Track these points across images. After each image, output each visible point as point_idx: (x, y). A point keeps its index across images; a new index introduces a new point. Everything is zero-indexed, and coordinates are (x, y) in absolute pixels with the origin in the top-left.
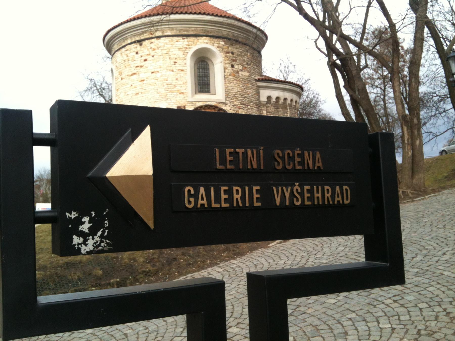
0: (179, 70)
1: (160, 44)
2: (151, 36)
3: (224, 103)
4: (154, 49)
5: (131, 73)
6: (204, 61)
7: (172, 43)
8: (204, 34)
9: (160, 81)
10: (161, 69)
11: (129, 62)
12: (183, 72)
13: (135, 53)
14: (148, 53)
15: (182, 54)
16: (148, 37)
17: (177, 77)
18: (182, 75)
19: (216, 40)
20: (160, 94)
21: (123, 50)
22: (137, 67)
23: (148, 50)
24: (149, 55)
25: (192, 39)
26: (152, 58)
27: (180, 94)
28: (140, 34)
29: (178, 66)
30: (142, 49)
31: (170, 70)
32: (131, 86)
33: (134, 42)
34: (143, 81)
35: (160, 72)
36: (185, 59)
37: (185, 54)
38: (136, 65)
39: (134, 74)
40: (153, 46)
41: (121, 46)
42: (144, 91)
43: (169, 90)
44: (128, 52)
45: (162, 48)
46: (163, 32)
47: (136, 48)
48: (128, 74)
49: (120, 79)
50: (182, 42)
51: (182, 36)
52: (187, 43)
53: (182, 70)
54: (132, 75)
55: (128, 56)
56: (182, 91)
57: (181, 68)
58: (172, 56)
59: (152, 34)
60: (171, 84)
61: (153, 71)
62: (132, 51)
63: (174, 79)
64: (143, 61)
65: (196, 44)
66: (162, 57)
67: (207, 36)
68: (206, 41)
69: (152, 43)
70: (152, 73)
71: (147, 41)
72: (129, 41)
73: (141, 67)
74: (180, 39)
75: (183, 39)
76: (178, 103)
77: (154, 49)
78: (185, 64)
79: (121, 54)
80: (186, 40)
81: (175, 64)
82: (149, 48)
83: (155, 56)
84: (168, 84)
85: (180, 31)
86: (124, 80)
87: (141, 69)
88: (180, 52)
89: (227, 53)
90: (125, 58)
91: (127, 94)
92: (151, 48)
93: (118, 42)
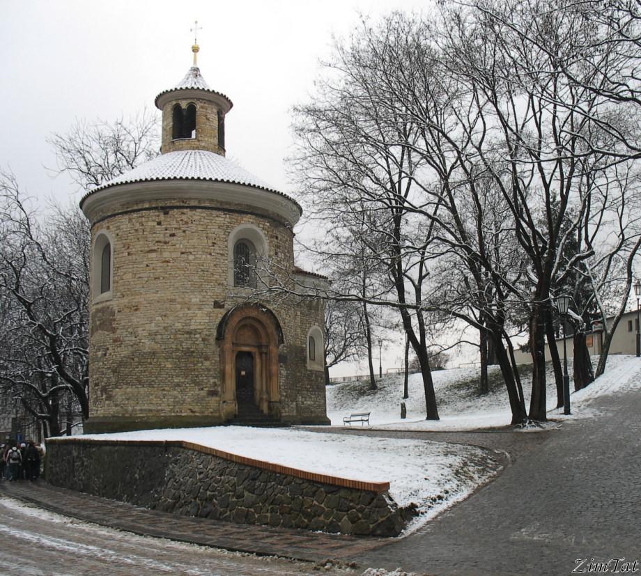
1: (195, 218)
2: (182, 204)
4: (186, 223)
5: (147, 249)
7: (211, 218)
8: (249, 211)
9: (193, 266)
10: (196, 250)
11: (145, 233)
13: (156, 223)
16: (178, 204)
20: (192, 283)
21: (135, 215)
22: (157, 242)
23: (177, 222)
24: (179, 229)
25: (235, 216)
26: (183, 234)
27: (219, 284)
28: (166, 199)
30: (169, 220)
32: (147, 266)
33: (156, 208)
34: (168, 262)
35: (193, 253)
36: (226, 241)
38: (157, 239)
40: (184, 217)
41: (129, 209)
42: (167, 276)
44: (143, 219)
45: (198, 223)
46: (199, 202)
47: (158, 216)
48: (143, 249)
50: (223, 219)
51: (224, 210)
52: (229, 220)
53: (222, 255)
55: (143, 225)
57: (221, 252)
58: (210, 235)
59: (183, 202)
60: (207, 271)
61: (183, 250)
63: (212, 265)
64: (168, 235)
65: (240, 223)
66: (196, 234)
67: (252, 214)
69: (183, 213)
70: (182, 253)
71: (175, 210)
72: (147, 206)
73: (166, 243)
77: (186, 223)
78: (226, 247)
79: (130, 219)
80: (228, 216)
81: (213, 246)
82: (179, 219)
83: (187, 232)
84: (203, 271)
85: (222, 203)
86: (134, 257)
88: (220, 230)
89: (272, 237)
90: (137, 226)
91: (139, 276)
92: (182, 220)
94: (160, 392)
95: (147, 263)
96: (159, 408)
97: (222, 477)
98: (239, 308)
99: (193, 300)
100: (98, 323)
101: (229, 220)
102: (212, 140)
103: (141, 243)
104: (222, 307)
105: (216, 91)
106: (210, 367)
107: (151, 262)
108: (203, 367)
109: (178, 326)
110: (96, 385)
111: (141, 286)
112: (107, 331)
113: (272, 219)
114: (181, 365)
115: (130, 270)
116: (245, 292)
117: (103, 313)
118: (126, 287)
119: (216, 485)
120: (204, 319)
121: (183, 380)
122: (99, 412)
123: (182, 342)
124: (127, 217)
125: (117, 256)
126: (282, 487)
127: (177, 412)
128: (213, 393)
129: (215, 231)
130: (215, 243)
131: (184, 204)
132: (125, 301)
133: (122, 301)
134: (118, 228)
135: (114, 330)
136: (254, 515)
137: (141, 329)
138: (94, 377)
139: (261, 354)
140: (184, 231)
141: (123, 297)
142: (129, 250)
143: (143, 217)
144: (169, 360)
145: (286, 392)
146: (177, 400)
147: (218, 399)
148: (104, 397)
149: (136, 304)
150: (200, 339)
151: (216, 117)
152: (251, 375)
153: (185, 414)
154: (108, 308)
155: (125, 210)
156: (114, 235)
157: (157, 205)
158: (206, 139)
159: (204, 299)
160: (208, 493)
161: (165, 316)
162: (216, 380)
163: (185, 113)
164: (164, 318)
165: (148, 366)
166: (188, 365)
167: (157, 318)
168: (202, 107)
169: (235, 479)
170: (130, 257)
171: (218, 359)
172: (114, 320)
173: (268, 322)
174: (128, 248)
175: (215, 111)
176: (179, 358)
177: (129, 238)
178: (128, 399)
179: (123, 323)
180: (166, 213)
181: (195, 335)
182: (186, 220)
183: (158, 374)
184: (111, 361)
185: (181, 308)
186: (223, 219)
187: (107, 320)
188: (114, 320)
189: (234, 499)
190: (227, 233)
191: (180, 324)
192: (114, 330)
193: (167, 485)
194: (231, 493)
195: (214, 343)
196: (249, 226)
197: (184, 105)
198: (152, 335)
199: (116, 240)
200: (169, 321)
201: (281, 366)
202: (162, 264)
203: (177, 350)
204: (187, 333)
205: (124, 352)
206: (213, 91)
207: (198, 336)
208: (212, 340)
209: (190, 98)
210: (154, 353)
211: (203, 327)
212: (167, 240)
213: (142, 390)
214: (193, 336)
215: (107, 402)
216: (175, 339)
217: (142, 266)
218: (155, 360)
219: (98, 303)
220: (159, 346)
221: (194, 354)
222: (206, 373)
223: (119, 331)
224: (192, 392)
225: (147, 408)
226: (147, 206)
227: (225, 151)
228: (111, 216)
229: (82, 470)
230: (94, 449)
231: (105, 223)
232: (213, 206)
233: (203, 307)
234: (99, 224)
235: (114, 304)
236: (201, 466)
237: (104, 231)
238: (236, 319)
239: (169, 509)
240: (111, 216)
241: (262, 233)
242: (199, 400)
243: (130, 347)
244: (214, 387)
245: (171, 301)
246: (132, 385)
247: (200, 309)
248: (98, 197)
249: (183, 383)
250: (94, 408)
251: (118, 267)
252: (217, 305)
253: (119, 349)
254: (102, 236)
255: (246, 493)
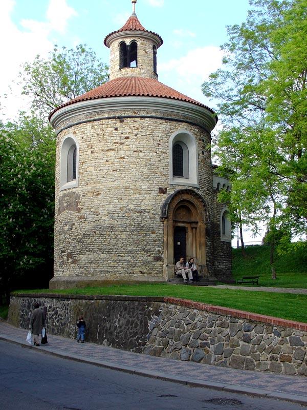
0: (162, 152)
2: (134, 115)
3: (198, 189)
4: (137, 129)
6: (179, 145)
12: (165, 155)
14: (130, 131)
15: (165, 136)
16: (131, 114)
17: (159, 159)
18: (165, 157)
19: (193, 127)
21: (96, 123)
22: (115, 143)
25: (174, 123)
27: (163, 175)
28: (121, 111)
29: (161, 149)
31: (153, 151)
32: (107, 161)
33: (114, 118)
34: (124, 158)
36: (168, 142)
37: (168, 137)
38: (115, 141)
39: (112, 150)
40: (135, 124)
41: (92, 119)
43: (152, 170)
45: (146, 129)
46: (147, 113)
47: (116, 124)
48: (103, 148)
49: (90, 152)
50: (165, 126)
51: (166, 119)
52: (169, 127)
54: (108, 150)
55: (103, 130)
56: (165, 173)
57: (164, 151)
59: (135, 113)
60: (154, 165)
61: (135, 149)
62: (109, 125)
68: (186, 127)
69: (135, 121)
70: (134, 151)
71: (129, 119)
73: (121, 144)
74: (163, 121)
75: (166, 122)
76: (160, 185)
77: (137, 129)
79: (93, 127)
80: (169, 124)
87: (121, 146)
88: (163, 134)
89: (200, 140)
90: (99, 131)
91: (100, 168)
92: (134, 127)
93: (88, 114)
94: (117, 258)
95: (107, 159)
96: (116, 269)
97: (213, 328)
98: (179, 193)
99: (143, 187)
100: (65, 205)
101: (169, 127)
102: (149, 68)
103: (102, 144)
104: (165, 192)
105: (153, 32)
106: (156, 238)
107: (110, 158)
108: (151, 239)
109: (132, 207)
110: (63, 252)
111: (102, 176)
112: (73, 211)
113: (201, 127)
114: (134, 237)
115: (93, 165)
116: (181, 183)
117: (70, 196)
118: (90, 177)
119: (207, 335)
120: (153, 202)
121: (135, 248)
122: (65, 273)
123: (134, 219)
124: (90, 124)
125: (82, 154)
126: (280, 339)
127: (130, 273)
128: (158, 259)
129: (158, 134)
130: (160, 144)
131: (136, 115)
132: (89, 187)
133: (86, 188)
134: (83, 133)
135: (79, 210)
136: (253, 362)
137: (102, 209)
138: (61, 246)
139: (192, 228)
140: (136, 135)
141: (87, 185)
142: (92, 150)
143: (103, 124)
144: (124, 233)
145: (210, 258)
146: (130, 263)
147: (161, 263)
148: (70, 261)
149: (98, 190)
150: (148, 217)
151: (152, 51)
152: (184, 244)
153: (136, 275)
154: (74, 193)
155: (89, 119)
156: (80, 138)
157: (114, 116)
158: (145, 67)
159: (151, 187)
160: (199, 341)
161: (121, 199)
162: (160, 249)
163: (128, 48)
164: (120, 201)
165: (107, 237)
166: (139, 237)
167: (115, 201)
168: (142, 44)
169: (228, 330)
170: (93, 155)
171: (162, 232)
172: (80, 202)
173: (199, 203)
174: (91, 148)
175: (151, 46)
176: (132, 232)
177: (92, 140)
178: (91, 263)
179: (87, 204)
180: (121, 122)
181: (144, 213)
182: (137, 126)
183: (115, 244)
184: (76, 234)
185: (134, 194)
186: (165, 126)
187: (74, 202)
188: (80, 202)
189: (229, 348)
190: (168, 137)
191: (133, 206)
192: (79, 210)
193: (151, 333)
194: (224, 342)
195: (158, 220)
196: (184, 131)
197: (128, 42)
198: (110, 214)
199: (81, 142)
200: (124, 203)
201: (206, 238)
202: (118, 160)
203: (131, 225)
204: (139, 212)
205: (87, 227)
206: (151, 32)
207: (146, 214)
208: (158, 218)
209: (133, 37)
210: (111, 228)
211: (151, 207)
212: (123, 141)
213: (102, 256)
214: (142, 214)
215: (73, 265)
216: (129, 217)
217: (102, 161)
218: (113, 233)
219: (65, 190)
220: (116, 222)
221: (144, 228)
222: (153, 243)
223: (83, 211)
224: (142, 258)
225: (106, 269)
226: (106, 116)
227: (157, 75)
228: (77, 124)
229: (56, 318)
230: (69, 302)
231: (71, 130)
232: (157, 116)
233: (150, 192)
234: (66, 130)
235: (79, 190)
236: (188, 318)
237: (71, 136)
238: (176, 202)
239: (157, 353)
240: (77, 124)
241: (193, 136)
242: (145, 264)
243: (93, 223)
244: (159, 254)
245: (127, 188)
246: (94, 252)
247: (148, 194)
248: (66, 110)
249: (134, 250)
250: (61, 269)
251: (83, 163)
252: (162, 191)
253: (83, 225)
254: (69, 140)
255: (241, 343)
